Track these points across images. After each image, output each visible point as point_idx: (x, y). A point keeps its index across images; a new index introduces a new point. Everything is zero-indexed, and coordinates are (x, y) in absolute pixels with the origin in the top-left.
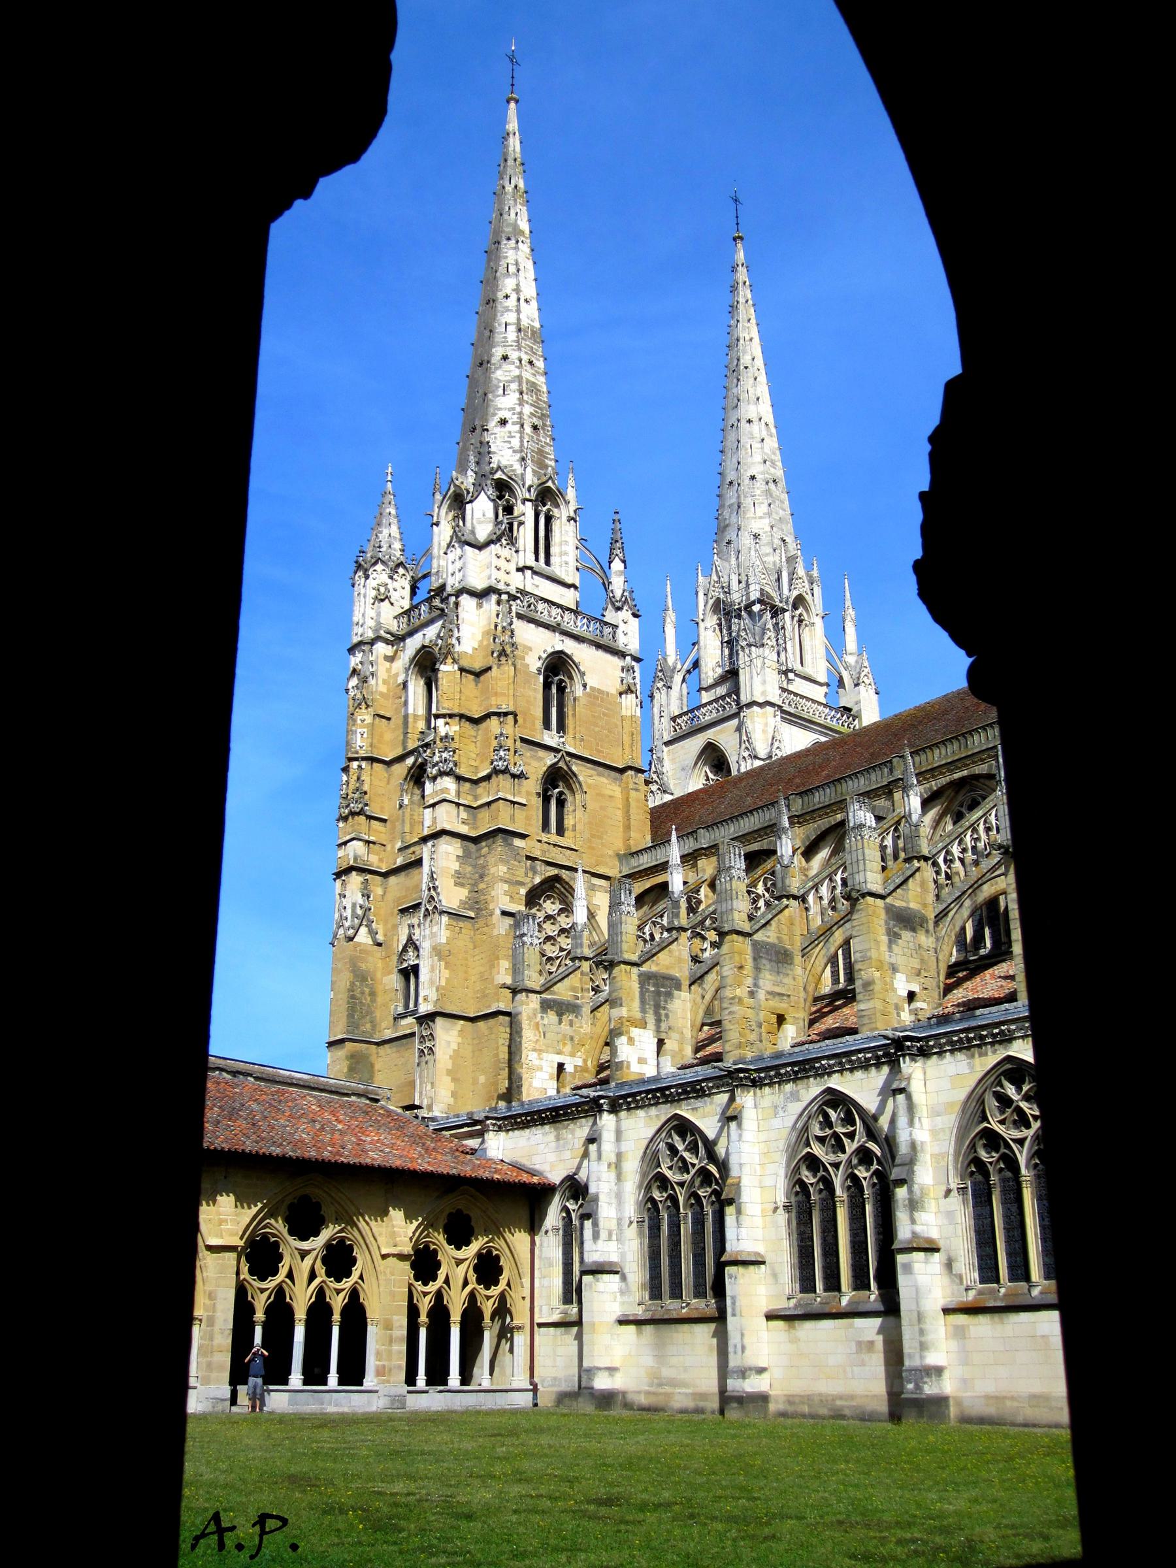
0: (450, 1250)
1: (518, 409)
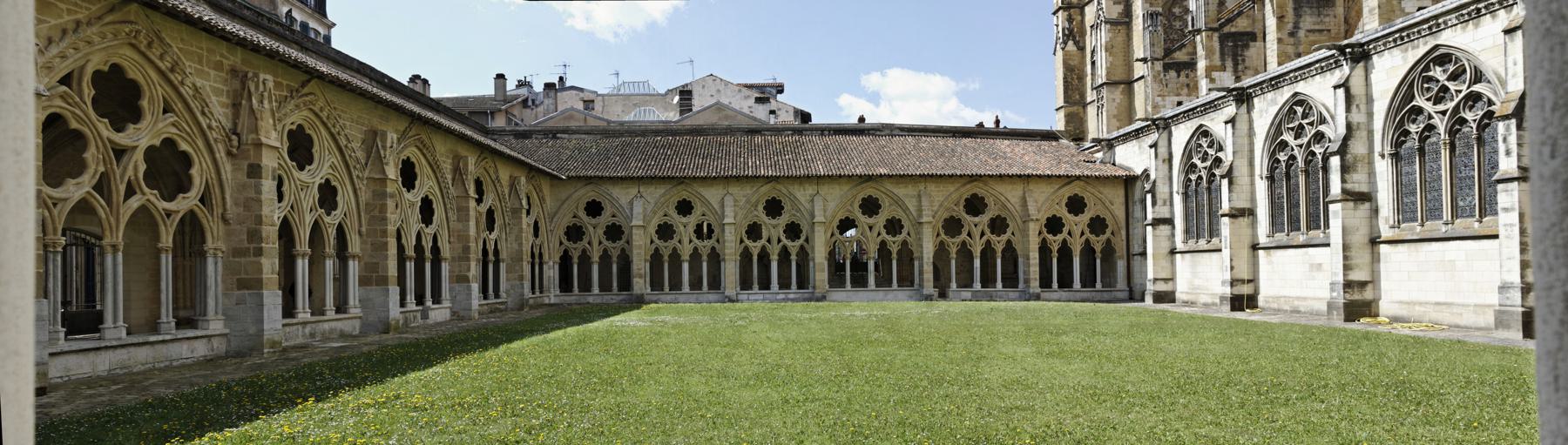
0: (1071, 217)
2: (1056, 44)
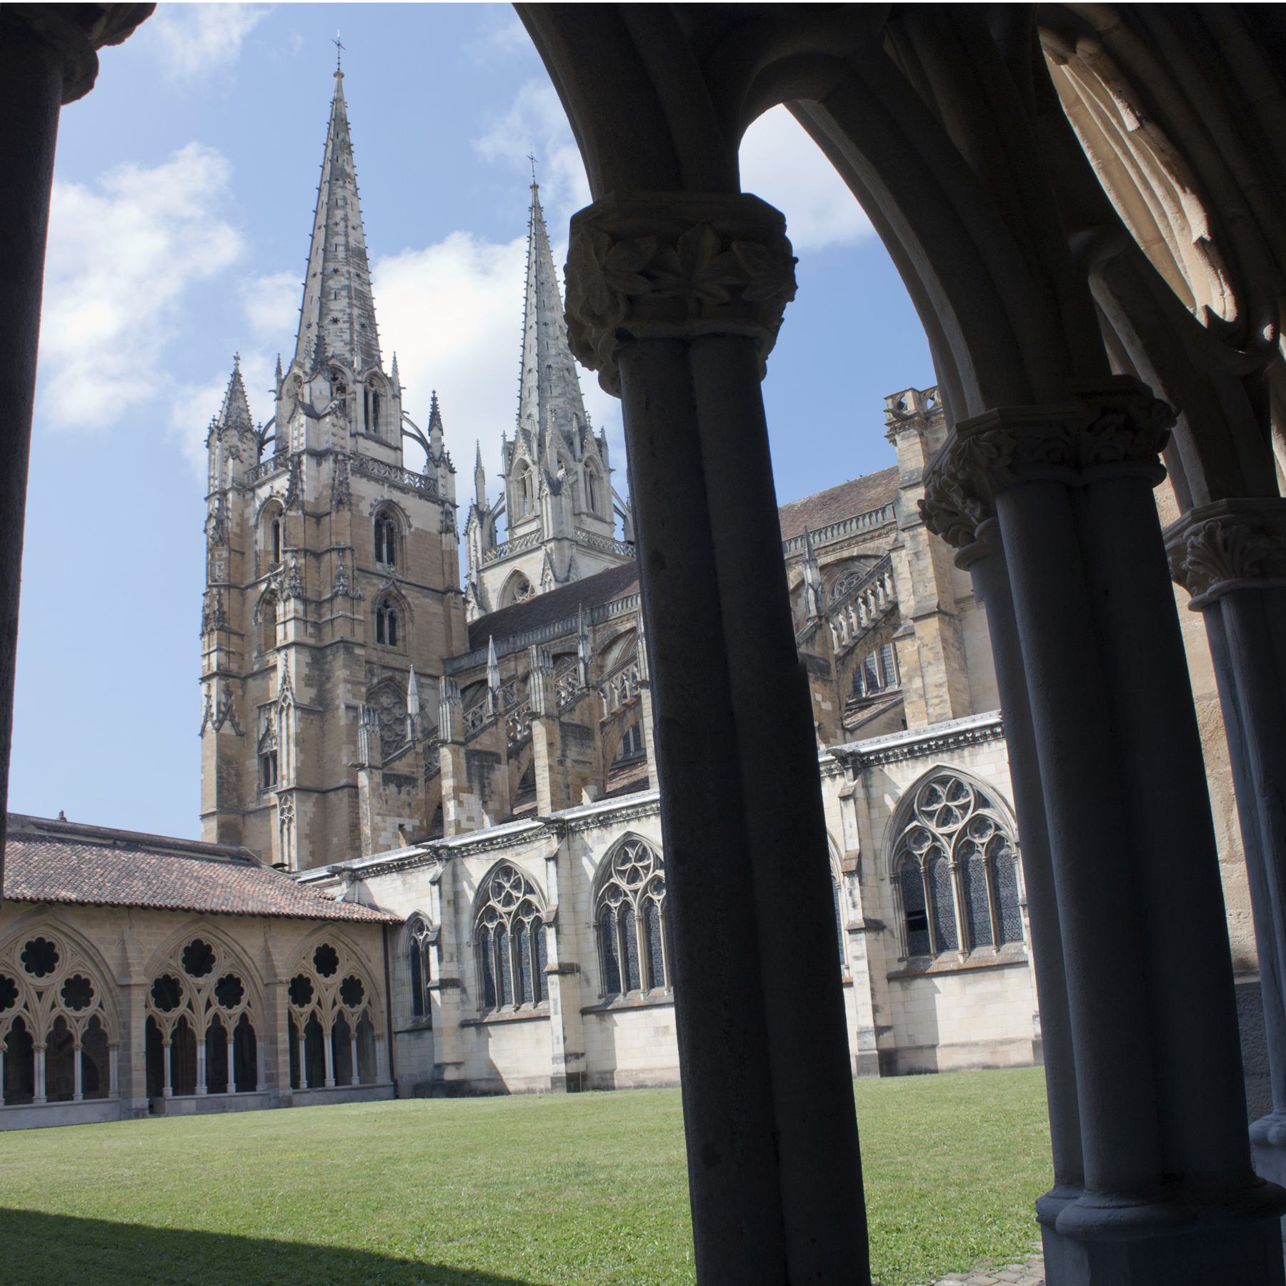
0: (320, 977)
1: (348, 311)
2: (206, 722)
